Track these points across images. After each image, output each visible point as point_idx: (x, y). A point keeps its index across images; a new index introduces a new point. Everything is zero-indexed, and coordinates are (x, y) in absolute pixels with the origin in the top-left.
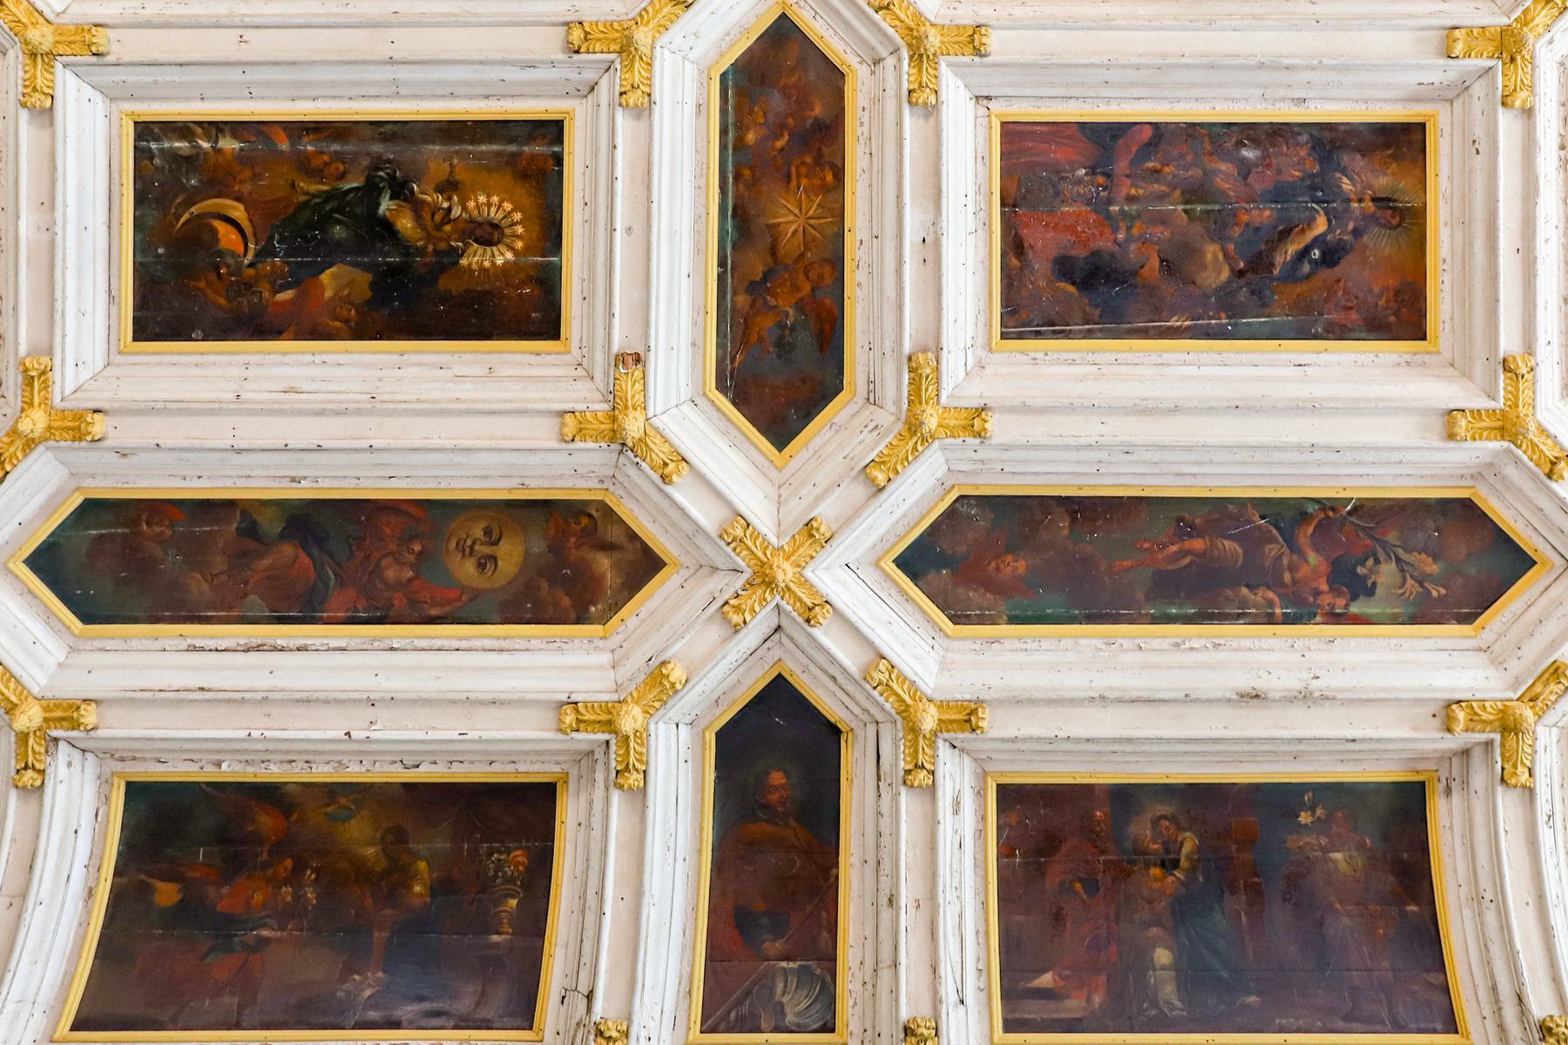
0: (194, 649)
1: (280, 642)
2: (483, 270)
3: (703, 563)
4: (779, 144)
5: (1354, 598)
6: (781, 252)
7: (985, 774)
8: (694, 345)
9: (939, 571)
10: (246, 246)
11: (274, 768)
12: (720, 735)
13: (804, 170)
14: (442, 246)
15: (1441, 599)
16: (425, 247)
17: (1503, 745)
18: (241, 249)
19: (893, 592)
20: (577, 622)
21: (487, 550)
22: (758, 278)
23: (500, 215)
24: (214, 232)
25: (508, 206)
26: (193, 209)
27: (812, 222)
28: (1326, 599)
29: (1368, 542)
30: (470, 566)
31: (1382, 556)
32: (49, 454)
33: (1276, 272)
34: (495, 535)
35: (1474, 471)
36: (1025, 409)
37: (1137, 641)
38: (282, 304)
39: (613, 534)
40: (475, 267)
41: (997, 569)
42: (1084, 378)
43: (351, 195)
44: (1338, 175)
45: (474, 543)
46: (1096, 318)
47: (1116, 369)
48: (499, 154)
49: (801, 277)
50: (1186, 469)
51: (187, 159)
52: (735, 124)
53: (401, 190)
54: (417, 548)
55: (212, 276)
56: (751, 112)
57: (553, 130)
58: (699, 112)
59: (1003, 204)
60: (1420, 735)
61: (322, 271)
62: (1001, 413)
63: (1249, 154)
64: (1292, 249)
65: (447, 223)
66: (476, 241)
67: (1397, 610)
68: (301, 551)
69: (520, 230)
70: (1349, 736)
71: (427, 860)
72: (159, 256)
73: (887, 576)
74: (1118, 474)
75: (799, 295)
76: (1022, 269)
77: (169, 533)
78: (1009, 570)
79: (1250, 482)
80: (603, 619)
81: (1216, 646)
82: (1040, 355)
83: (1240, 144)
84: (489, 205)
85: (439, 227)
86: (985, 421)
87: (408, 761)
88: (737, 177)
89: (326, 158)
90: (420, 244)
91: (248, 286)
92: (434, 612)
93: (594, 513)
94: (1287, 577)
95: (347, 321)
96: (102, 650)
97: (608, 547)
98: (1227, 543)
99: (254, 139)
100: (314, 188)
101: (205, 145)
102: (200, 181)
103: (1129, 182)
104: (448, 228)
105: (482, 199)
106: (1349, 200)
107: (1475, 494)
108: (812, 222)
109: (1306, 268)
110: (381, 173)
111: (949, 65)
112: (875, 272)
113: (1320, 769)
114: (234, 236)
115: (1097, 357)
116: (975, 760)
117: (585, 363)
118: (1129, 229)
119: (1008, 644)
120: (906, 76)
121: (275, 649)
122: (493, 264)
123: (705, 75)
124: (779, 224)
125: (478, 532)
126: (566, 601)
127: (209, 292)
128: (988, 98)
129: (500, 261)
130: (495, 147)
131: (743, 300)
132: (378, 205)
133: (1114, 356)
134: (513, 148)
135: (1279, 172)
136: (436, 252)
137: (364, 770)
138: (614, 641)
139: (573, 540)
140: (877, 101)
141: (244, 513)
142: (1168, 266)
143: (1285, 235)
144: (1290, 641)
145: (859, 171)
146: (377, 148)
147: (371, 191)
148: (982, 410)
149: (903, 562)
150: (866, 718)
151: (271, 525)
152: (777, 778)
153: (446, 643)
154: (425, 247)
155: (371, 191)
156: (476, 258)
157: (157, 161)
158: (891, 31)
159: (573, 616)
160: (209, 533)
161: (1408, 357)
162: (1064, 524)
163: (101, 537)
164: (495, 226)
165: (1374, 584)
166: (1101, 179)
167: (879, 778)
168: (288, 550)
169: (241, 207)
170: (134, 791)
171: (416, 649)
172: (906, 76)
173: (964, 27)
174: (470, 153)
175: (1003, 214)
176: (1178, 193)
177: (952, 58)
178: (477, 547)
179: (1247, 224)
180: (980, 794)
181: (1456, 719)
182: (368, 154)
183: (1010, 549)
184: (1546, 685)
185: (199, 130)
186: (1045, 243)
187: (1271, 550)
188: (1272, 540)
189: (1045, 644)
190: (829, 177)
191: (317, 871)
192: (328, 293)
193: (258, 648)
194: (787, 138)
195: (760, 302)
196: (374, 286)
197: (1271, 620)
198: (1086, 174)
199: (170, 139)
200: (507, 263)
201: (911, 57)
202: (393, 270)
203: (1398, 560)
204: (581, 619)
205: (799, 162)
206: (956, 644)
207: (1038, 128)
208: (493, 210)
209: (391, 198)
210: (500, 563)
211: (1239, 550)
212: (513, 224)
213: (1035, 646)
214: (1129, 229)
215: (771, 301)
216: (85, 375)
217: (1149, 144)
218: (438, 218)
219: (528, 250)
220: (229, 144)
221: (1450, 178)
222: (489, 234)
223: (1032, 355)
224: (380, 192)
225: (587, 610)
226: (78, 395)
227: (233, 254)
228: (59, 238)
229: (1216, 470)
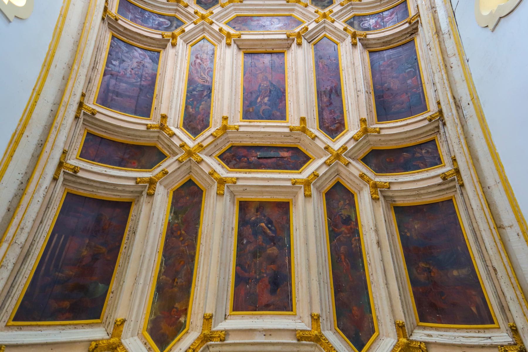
5: (351, 220)
15: (349, 201)
17: (380, 188)
31: (340, 213)
36: (311, 303)
42: (302, 286)
46: (286, 283)
47: (299, 277)
50: (324, 259)
60: (381, 205)
62: (312, 310)
63: (245, 242)
64: (269, 231)
70: (384, 221)
79: (325, 243)
83: (242, 244)
86: (314, 315)
94: (348, 235)
106: (257, 218)
107: (324, 192)
109: (273, 228)
115: (296, 282)
118: (263, 273)
133: (296, 277)
135: (250, 234)
143: (265, 233)
148: (311, 315)
161: (293, 206)
166: (250, 281)
176: (254, 260)
179: (263, 242)
181: (375, 197)
184: (365, 179)
186: (266, 298)
187: (342, 239)
188: (339, 238)
203: (341, 210)
207: (235, 300)
221: (252, 196)
229: (323, 251)
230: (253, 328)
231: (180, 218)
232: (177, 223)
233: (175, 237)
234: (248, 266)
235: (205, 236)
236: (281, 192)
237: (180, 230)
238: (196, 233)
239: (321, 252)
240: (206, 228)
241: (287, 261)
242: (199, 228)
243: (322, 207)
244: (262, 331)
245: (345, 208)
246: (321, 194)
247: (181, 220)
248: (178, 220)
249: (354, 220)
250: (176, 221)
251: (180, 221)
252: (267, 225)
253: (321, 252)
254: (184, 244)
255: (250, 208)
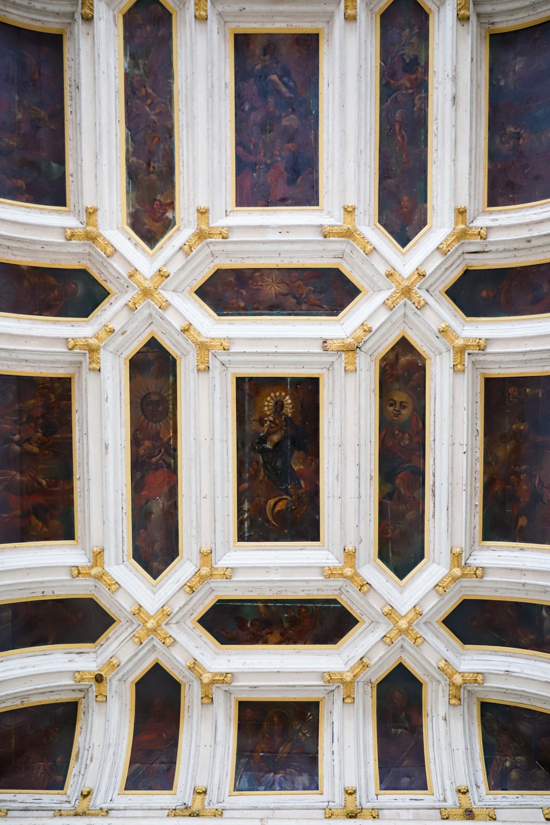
0: (434, 516)
1: (431, 483)
2: (293, 408)
3: (403, 320)
4: (245, 293)
5: (418, 64)
6: (286, 292)
7: (483, 211)
8: (321, 324)
9: (406, 231)
10: (284, 499)
11: (478, 485)
12: (468, 315)
13: (254, 284)
14: (284, 424)
15: (419, 28)
16: (284, 430)
18: (285, 501)
19: (415, 248)
20: (425, 370)
21: (398, 405)
22: (295, 301)
23: (272, 401)
24: (279, 511)
25: (269, 398)
26: (271, 519)
27: (274, 280)
28: (419, 75)
29: (397, 58)
30: (404, 412)
31: (402, 52)
32: (361, 569)
33: (293, 96)
34: (392, 402)
35: (369, 13)
37: (434, 151)
38: (306, 485)
39: (392, 357)
40: (292, 411)
41: (406, 208)
43: (265, 459)
44: (255, 70)
45: (395, 410)
46: (311, 169)
48: (249, 403)
49: (295, 284)
51: (251, 522)
52: (237, 311)
53: (263, 440)
54: (397, 432)
55: (295, 512)
56: (233, 304)
57: (240, 381)
58: (232, 324)
59: (267, 206)
61: (294, 470)
63: (247, 107)
64: (284, 89)
65: (275, 421)
66: (282, 411)
67: (424, 46)
68: (399, 476)
69: (278, 394)
71: (512, 425)
72: (288, 532)
73: (408, 250)
74: (370, 159)
75: (302, 285)
76: (292, 199)
77: (391, 527)
78: (407, 203)
80: (424, 360)
81: (436, 119)
82: (325, 190)
83: (243, 110)
84: (268, 406)
85: (277, 425)
87: (475, 434)
88: (257, 309)
89: (251, 469)
90: (283, 432)
91: (299, 498)
92: (421, 425)
93: (385, 363)
94: (410, 91)
95: (312, 460)
96: (434, 551)
97: (397, 358)
98: (397, 115)
99: (244, 497)
100: (262, 473)
101: (246, 515)
102: (260, 517)
103: (258, 156)
104: (277, 422)
105: (266, 409)
108: (274, 280)
109: (291, 84)
110: (257, 448)
111: (213, 223)
112: (293, 255)
113: (484, 77)
114: (280, 503)
116: (478, 216)
117: (328, 366)
118: (276, 156)
119: (434, 203)
120: (217, 240)
121: (434, 485)
122: (290, 404)
123: (218, 322)
124: (275, 294)
125: (391, 409)
126: (417, 375)
127: (301, 513)
128: (226, 211)
129: (289, 401)
130: (246, 404)
131: (304, 307)
132: (269, 449)
134: (247, 397)
136: (286, 426)
137: (479, 451)
138: (432, 355)
139: (394, 372)
140: (228, 254)
141: (383, 498)
142: (291, 139)
144: (434, 89)
145: (255, 262)
146: (247, 449)
147: (264, 451)
149: (403, 245)
150: (462, 258)
151: (389, 488)
152: (484, 294)
153: (432, 420)
154: (284, 430)
155: (264, 451)
156: (288, 410)
157: (252, 533)
158: (200, 246)
159: (423, 372)
160: (391, 510)
161: (325, 40)
162: (389, 181)
163: (392, 552)
164: (276, 403)
165: (413, 55)
166: (258, 167)
167: (484, 252)
168: (398, 481)
169: (269, 501)
170: (486, 537)
171: (434, 431)
172: (217, 240)
173: (198, 217)
174: (249, 414)
175: (271, 206)
176: (263, 136)
177: (210, 222)
178: (397, 409)
179: (274, 107)
180: (491, 213)
182: (249, 453)
183: (399, 202)
185: (241, 517)
188: (396, 97)
189: (435, 188)
190: (257, 274)
191: (515, 466)
192: (302, 467)
193: (433, 492)
194: (242, 290)
195: (305, 300)
196: (299, 449)
197: (427, 98)
198: (256, 173)
199: (244, 528)
200: (290, 399)
201: (210, 238)
202: (293, 442)
204: (423, 369)
205: (251, 286)
206: (434, 223)
208: (270, 404)
209: (266, 443)
210: (403, 400)
211: (399, 111)
212: (276, 396)
213: (435, 192)
214: (276, 156)
215: (304, 295)
216: (332, 556)
217: (244, 148)
218: (273, 425)
219: (285, 390)
220: (246, 506)
221: (255, 22)
222: (279, 405)
223: (324, 193)
224: (264, 448)
225: (421, 366)
226: (339, 559)
227: (287, 504)
228: (280, 565)
229: (368, 119)
230: (265, 224)
231: (141, 66)
232: (138, 75)
233: (138, 98)
234: (254, 146)
235: (184, 97)
236: (304, 12)
237: (145, 87)
238: (170, 93)
239: (365, 119)
240: (184, 83)
241: (312, 137)
242: (173, 83)
243: (374, 41)
244: (277, 228)
245: (411, 43)
246: (374, 15)
247: (144, 70)
248: (139, 68)
249: (423, 64)
250: (137, 72)
251: (142, 71)
252: (280, 78)
253: (365, 119)
254: (154, 110)
255: (252, 47)
